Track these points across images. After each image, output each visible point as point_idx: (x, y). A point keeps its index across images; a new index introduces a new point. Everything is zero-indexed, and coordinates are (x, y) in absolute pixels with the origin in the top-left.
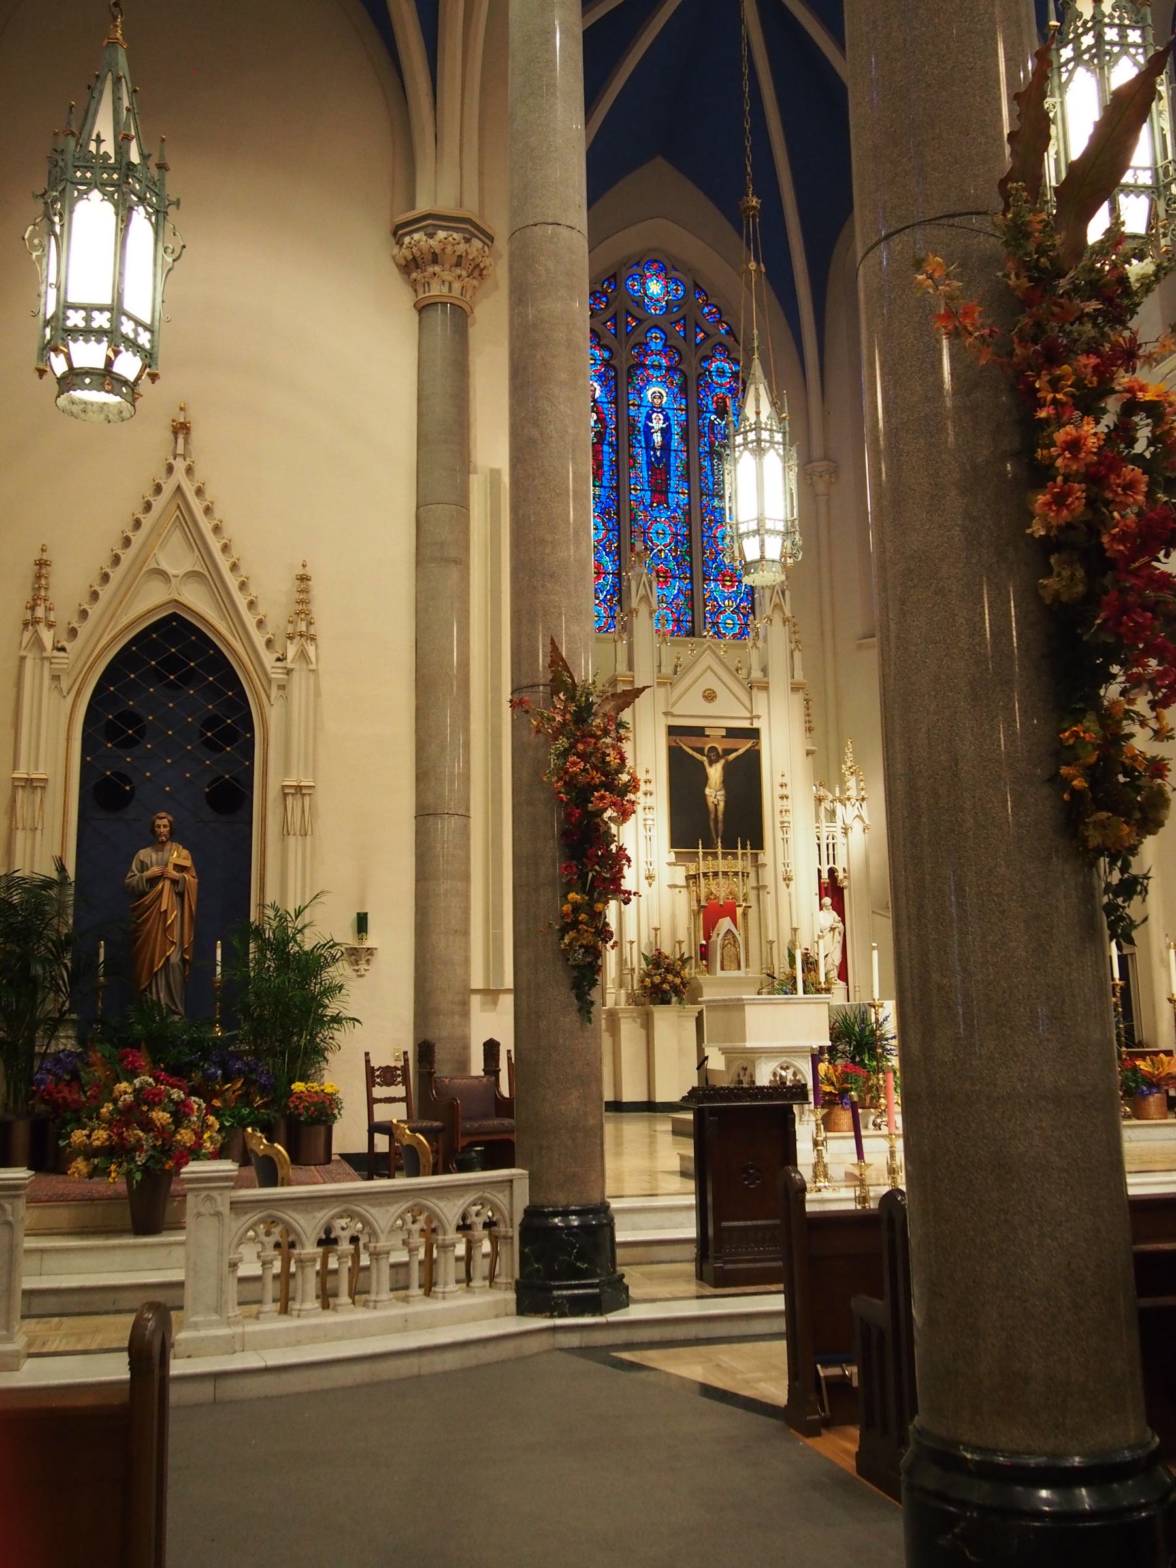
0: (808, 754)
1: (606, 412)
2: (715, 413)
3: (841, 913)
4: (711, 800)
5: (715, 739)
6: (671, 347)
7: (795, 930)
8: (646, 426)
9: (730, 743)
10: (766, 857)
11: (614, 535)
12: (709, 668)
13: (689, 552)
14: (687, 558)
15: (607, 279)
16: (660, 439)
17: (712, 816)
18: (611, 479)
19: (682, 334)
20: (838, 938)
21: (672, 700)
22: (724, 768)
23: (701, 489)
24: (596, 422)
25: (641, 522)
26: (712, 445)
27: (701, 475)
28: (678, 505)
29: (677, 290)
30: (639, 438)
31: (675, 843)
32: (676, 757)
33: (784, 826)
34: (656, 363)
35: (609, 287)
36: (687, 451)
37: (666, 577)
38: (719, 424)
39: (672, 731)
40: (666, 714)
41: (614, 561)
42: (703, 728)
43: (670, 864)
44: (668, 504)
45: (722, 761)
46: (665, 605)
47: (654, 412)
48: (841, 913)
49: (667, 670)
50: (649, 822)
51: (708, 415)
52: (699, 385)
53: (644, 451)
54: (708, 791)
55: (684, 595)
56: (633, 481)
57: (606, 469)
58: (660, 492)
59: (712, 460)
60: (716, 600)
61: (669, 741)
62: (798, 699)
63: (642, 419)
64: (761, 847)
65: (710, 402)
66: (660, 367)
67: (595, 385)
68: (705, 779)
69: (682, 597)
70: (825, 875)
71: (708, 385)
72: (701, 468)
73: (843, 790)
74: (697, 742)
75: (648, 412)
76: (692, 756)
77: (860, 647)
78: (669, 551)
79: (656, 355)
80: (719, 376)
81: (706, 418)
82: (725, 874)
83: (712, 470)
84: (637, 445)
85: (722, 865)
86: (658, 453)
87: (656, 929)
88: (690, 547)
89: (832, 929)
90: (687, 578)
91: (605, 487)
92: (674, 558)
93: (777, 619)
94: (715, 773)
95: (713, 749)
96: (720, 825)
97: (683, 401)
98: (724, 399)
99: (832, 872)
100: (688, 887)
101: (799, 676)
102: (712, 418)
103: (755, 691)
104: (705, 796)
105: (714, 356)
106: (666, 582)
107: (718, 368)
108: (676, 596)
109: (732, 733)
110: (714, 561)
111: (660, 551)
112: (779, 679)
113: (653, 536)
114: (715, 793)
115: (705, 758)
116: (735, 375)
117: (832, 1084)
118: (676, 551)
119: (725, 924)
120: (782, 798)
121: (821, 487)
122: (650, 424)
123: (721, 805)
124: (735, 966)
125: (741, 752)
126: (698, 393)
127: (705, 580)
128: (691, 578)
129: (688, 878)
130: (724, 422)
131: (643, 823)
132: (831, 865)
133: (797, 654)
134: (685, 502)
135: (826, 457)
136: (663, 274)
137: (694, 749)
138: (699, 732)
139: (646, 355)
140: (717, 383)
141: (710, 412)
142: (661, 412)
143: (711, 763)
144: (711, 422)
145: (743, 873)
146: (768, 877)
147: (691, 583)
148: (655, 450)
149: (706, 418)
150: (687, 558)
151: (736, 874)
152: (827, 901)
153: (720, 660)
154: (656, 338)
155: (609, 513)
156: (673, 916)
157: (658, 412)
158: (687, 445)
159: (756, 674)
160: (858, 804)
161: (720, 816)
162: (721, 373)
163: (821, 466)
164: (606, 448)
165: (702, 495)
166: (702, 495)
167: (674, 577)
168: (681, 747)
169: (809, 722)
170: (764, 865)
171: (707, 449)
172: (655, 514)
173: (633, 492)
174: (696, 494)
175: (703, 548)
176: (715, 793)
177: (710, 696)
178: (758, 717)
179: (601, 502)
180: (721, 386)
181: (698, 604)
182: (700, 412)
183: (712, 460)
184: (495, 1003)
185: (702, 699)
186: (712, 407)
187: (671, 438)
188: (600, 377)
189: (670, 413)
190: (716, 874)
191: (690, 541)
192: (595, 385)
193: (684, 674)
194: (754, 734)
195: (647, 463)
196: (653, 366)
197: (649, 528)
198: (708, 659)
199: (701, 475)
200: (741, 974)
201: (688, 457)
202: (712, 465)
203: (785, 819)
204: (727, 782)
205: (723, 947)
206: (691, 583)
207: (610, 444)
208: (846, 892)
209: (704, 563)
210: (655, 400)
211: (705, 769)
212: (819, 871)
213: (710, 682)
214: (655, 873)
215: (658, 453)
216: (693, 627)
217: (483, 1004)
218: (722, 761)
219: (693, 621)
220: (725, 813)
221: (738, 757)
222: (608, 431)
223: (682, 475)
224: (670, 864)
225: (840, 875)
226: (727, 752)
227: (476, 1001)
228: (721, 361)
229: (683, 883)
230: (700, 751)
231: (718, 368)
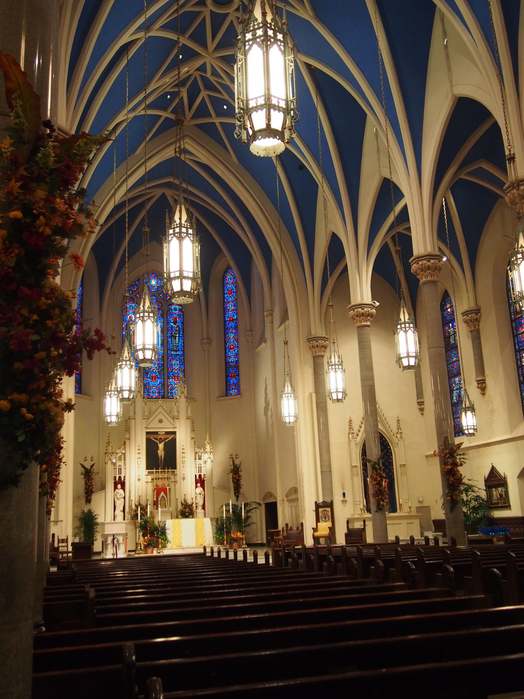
0: (192, 439)
2: (173, 323)
3: (204, 489)
4: (160, 455)
5: (162, 435)
6: (158, 302)
7: (185, 495)
9: (166, 436)
10: (177, 471)
12: (161, 412)
13: (163, 370)
15: (137, 280)
17: (160, 460)
19: (162, 297)
20: (203, 497)
21: (148, 424)
22: (164, 444)
23: (168, 348)
26: (172, 333)
27: (168, 344)
31: (147, 469)
32: (148, 441)
33: (183, 462)
35: (138, 283)
39: (148, 433)
40: (146, 428)
42: (158, 432)
43: (146, 475)
45: (164, 442)
48: (204, 489)
49: (147, 414)
50: (139, 463)
51: (171, 324)
52: (168, 314)
54: (159, 452)
55: (161, 384)
59: (171, 339)
60: (172, 385)
61: (146, 437)
62: (189, 422)
64: (176, 468)
67: (133, 316)
68: (158, 448)
69: (160, 385)
70: (198, 477)
71: (171, 314)
72: (168, 341)
73: (205, 449)
74: (156, 436)
76: (154, 441)
77: (217, 400)
82: (161, 478)
83: (172, 342)
85: (160, 476)
87: (140, 496)
88: (164, 368)
89: (200, 494)
90: (162, 378)
93: (183, 396)
94: (161, 446)
95: (161, 438)
96: (162, 462)
97: (162, 320)
98: (176, 318)
99: (200, 476)
100: (152, 482)
101: (190, 414)
103: (175, 419)
104: (158, 453)
106: (155, 380)
108: (159, 384)
109: (167, 433)
110: (172, 372)
111: (153, 370)
112: (183, 415)
114: (161, 452)
115: (158, 441)
116: (180, 310)
117: (146, 542)
118: (159, 369)
119: (162, 494)
120: (183, 453)
121: (206, 347)
123: (163, 456)
124: (164, 507)
125: (170, 439)
126: (167, 316)
127: (168, 378)
128: (164, 378)
129: (153, 479)
131: (137, 462)
132: (200, 473)
133: (189, 407)
134: (162, 353)
135: (208, 338)
136: (156, 278)
137: (154, 439)
138: (156, 433)
143: (160, 443)
144: (172, 326)
145: (167, 478)
146: (178, 478)
147: (164, 379)
151: (165, 478)
152: (199, 485)
153: (165, 411)
156: (147, 491)
158: (163, 334)
159: (176, 414)
160: (209, 454)
161: (163, 459)
162: (175, 309)
163: (205, 341)
165: (168, 350)
166: (168, 350)
167: (158, 378)
168: (150, 438)
169: (193, 428)
170: (177, 475)
171: (170, 335)
174: (166, 351)
175: (168, 368)
176: (161, 452)
177: (161, 421)
178: (176, 428)
180: (175, 314)
181: (166, 386)
182: (168, 323)
183: (171, 339)
184: (57, 524)
185: (158, 423)
186: (172, 321)
190: (159, 478)
191: (163, 366)
192: (133, 316)
193: (153, 414)
194: (174, 433)
198: (160, 409)
199: (168, 344)
200: (166, 509)
201: (163, 338)
202: (172, 340)
203: (183, 460)
204: (165, 449)
205: (161, 501)
206: (164, 379)
208: (205, 481)
209: (168, 373)
211: (158, 445)
212: (196, 476)
213: (160, 417)
214: (141, 478)
216: (164, 394)
217: (54, 524)
218: (164, 442)
219: (164, 392)
220: (164, 458)
221: (169, 441)
224: (146, 475)
225: (203, 477)
226: (165, 439)
227: (52, 524)
229: (150, 480)
230: (157, 439)
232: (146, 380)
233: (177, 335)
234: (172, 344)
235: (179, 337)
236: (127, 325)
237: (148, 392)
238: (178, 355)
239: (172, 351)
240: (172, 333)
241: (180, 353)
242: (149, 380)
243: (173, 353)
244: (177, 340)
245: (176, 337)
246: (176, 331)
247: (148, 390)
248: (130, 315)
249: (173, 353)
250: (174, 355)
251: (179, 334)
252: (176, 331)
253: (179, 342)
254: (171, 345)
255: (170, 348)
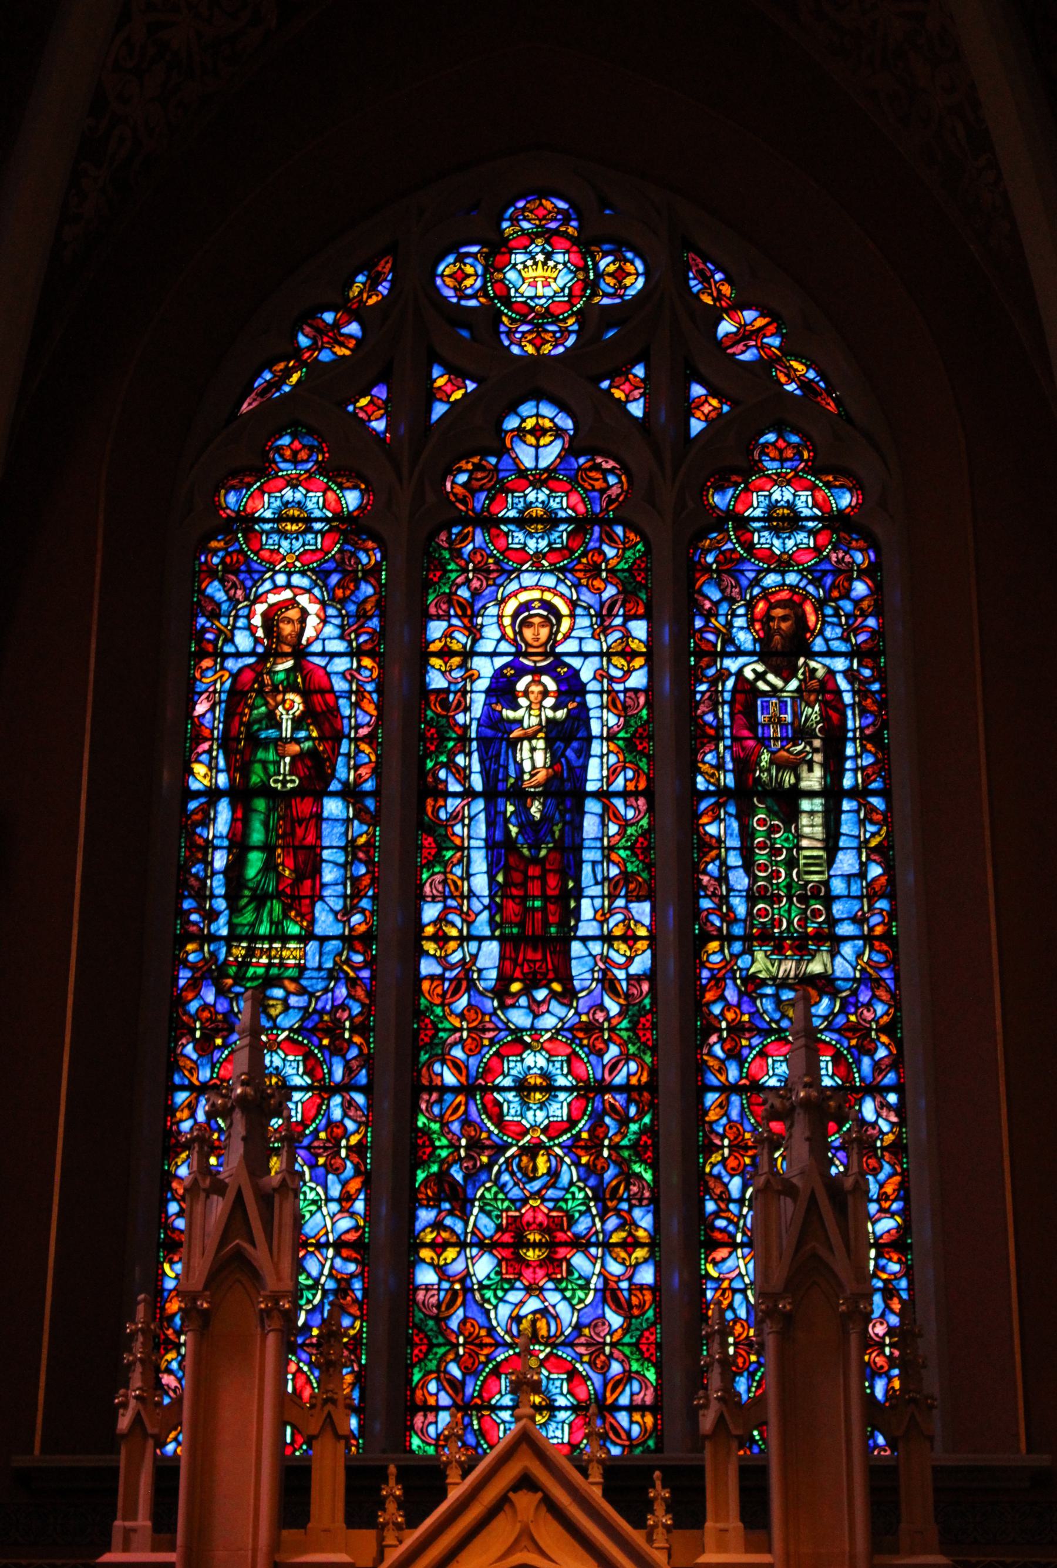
1: (339, 685)
8: (491, 720)
11: (348, 1106)
14: (637, 1168)
16: (540, 758)
18: (347, 913)
24: (298, 723)
25: (458, 1053)
28: (609, 984)
29: (620, 275)
30: (460, 760)
34: (538, 511)
35: (372, 286)
36: (648, 794)
37: (551, 1246)
38: (775, 691)
41: (346, 1199)
44: (567, 979)
46: (544, 1352)
47: (522, 671)
51: (732, 665)
53: (479, 805)
56: (430, 912)
57: (329, 874)
58: (540, 941)
63: (478, 703)
65: (740, 622)
66: (550, 521)
67: (303, 600)
69: (615, 1320)
75: (498, 674)
78: (568, 1149)
79: (538, 484)
80: (777, 532)
81: (723, 675)
84: (454, 787)
86: (535, 809)
90: (630, 1244)
91: (323, 939)
92: (590, 1171)
97: (639, 629)
102: (749, 674)
105: (756, 468)
107: (772, 507)
113: (511, 1105)
118: (594, 1146)
122: (509, 714)
130: (794, 684)
139: (501, 490)
140: (769, 555)
141: (739, 653)
142: (548, 670)
144: (746, 690)
148: (520, 795)
149: (723, 675)
150: (637, 1168)
154: (538, 431)
155: (334, 1030)
157: (536, 672)
164: (333, 807)
167: (581, 1244)
172: (519, 1018)
173: (430, 947)
179: (302, 991)
180: (782, 564)
183: (744, 816)
187: (585, 754)
188: (321, 575)
189: (587, 671)
195: (490, 844)
196: (523, 522)
197: (489, 1071)
207: (350, 794)
210: (528, 633)
215: (535, 809)
222: (344, 748)
223: (626, 876)
228: (781, 480)
231: (772, 507)
232: (441, 1270)
233: (813, 780)
234: (748, 865)
235: (832, 794)
236: (237, 697)
237: (463, 1407)
238: (825, 984)
239: (747, 939)
240: (745, 766)
241: (842, 968)
242: (484, 1267)
243: (760, 963)
244: (812, 827)
245: (797, 793)
246: (802, 733)
247: (456, 1387)
248: (273, 599)
249: (760, 963)
250: (781, 984)
251: (834, 767)
252: (802, 733)
253: (831, 845)
254: (739, 880)
255: (729, 918)
